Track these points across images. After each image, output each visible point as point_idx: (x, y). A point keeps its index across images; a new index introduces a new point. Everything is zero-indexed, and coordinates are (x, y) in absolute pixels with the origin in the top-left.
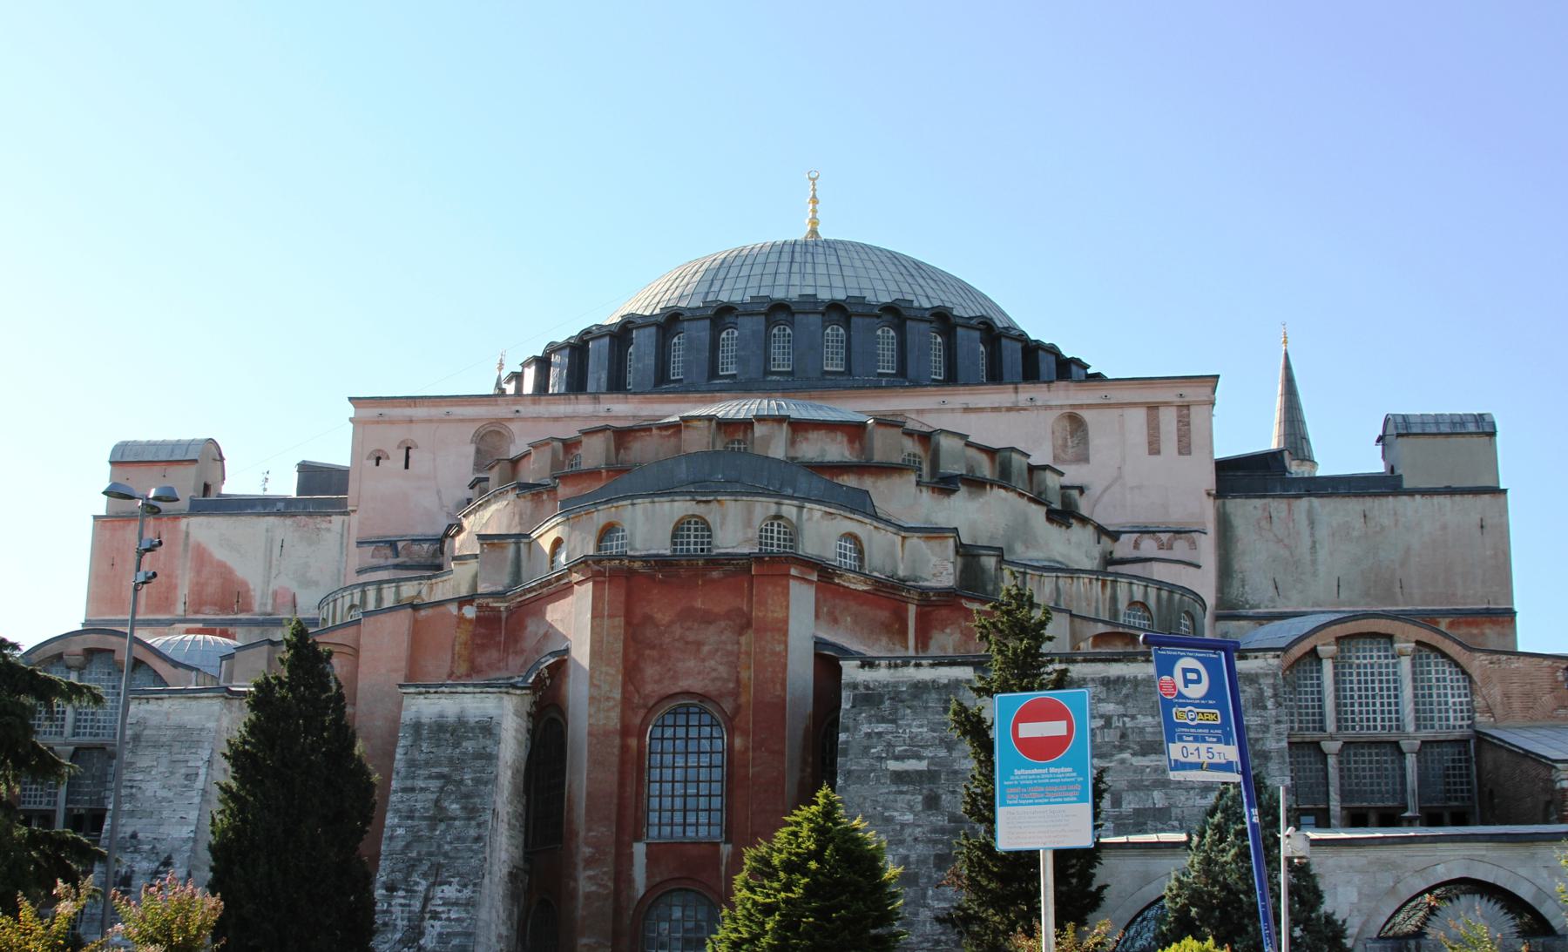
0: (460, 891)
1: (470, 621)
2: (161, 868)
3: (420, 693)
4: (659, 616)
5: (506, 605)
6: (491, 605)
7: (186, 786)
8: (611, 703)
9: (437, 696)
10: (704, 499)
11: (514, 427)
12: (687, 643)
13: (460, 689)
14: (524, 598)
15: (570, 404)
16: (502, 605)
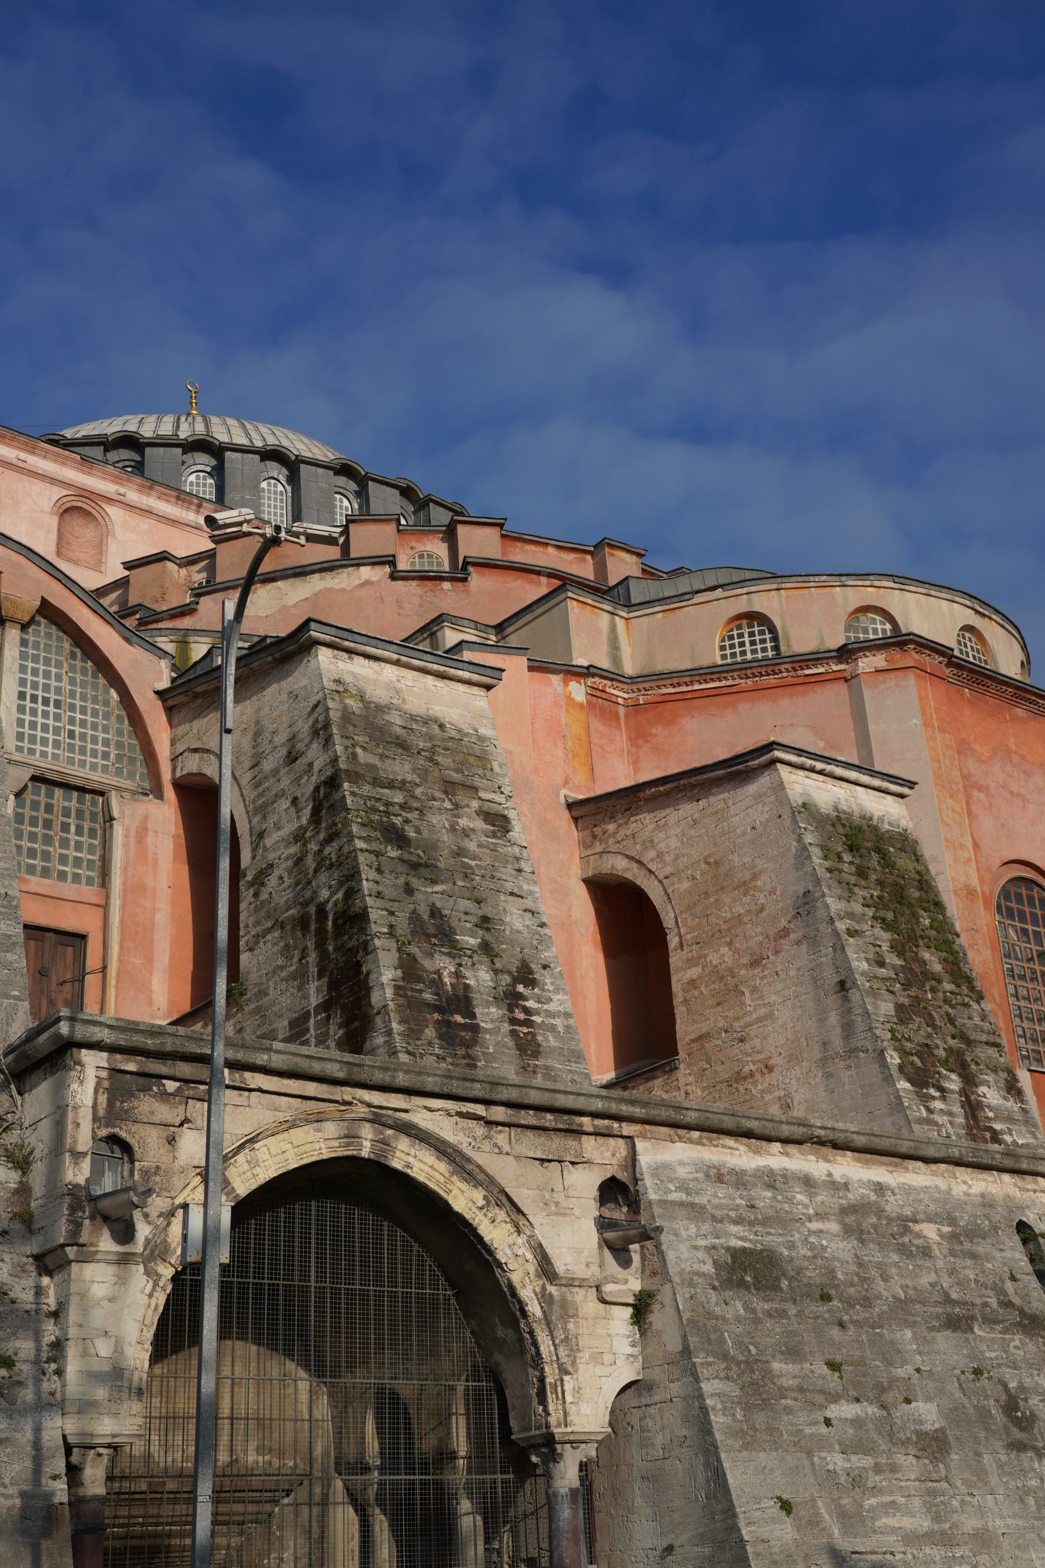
0: (1005, 1098)
1: (581, 706)
2: (520, 988)
3: (801, 767)
4: (977, 746)
5: (626, 696)
6: (608, 690)
7: (494, 835)
8: (966, 854)
9: (821, 778)
10: (982, 610)
11: (114, 512)
12: (1012, 793)
13: (853, 775)
14: (684, 689)
15: (188, 509)
16: (619, 694)
